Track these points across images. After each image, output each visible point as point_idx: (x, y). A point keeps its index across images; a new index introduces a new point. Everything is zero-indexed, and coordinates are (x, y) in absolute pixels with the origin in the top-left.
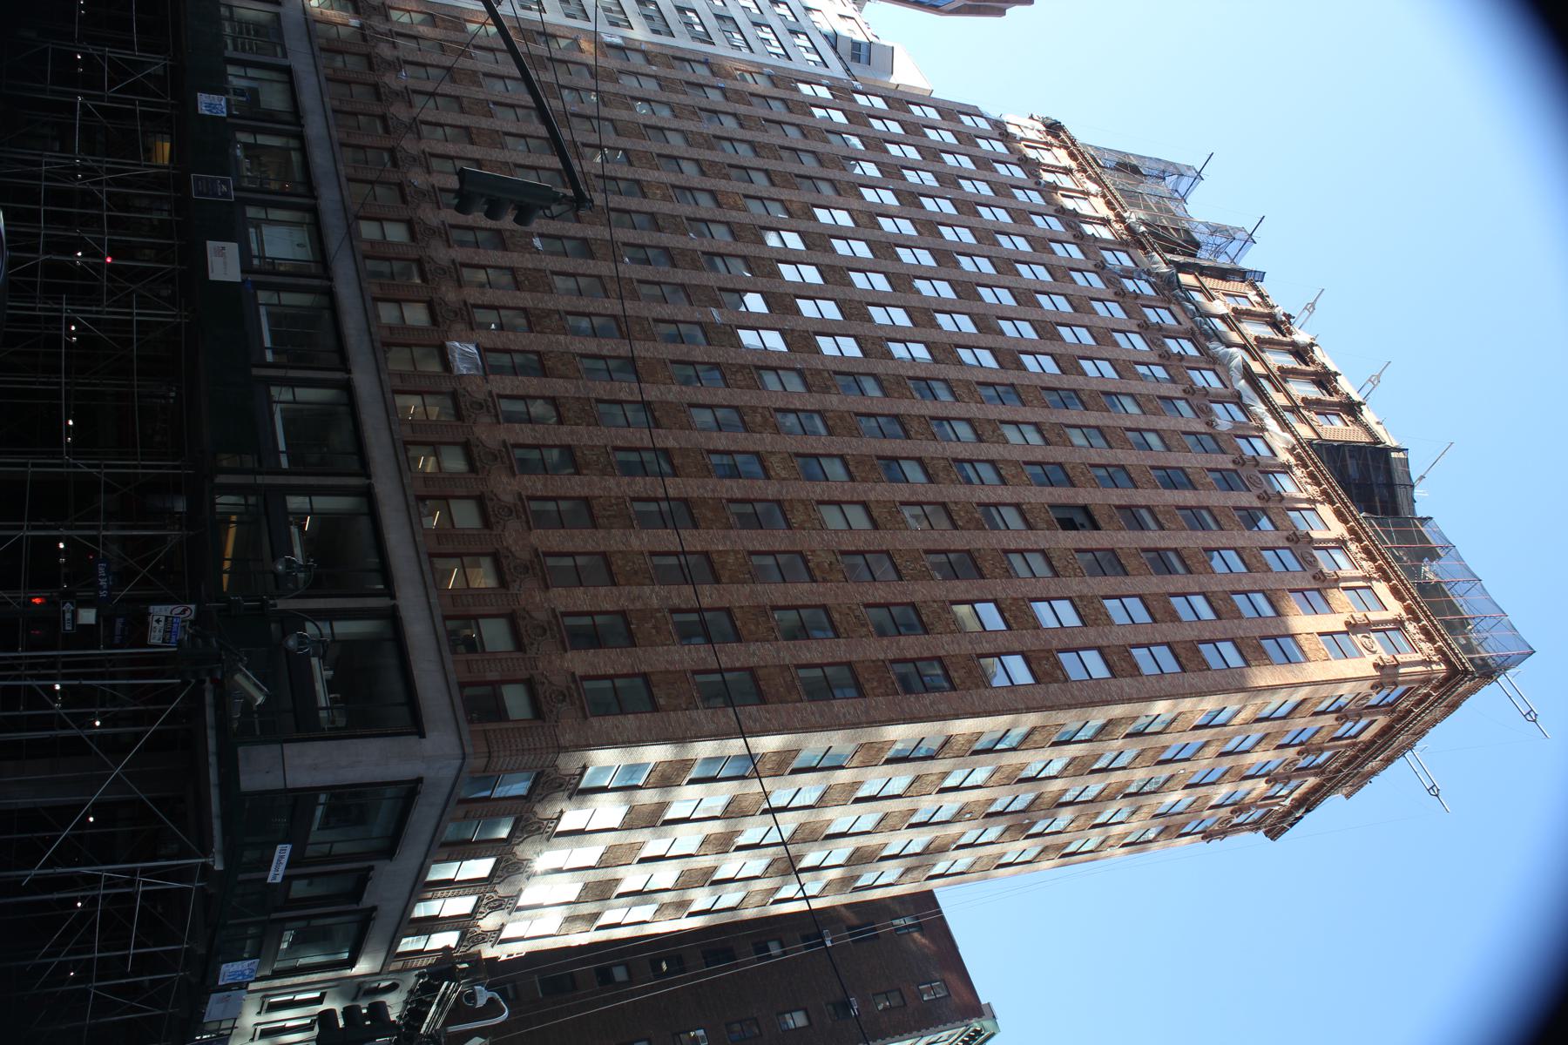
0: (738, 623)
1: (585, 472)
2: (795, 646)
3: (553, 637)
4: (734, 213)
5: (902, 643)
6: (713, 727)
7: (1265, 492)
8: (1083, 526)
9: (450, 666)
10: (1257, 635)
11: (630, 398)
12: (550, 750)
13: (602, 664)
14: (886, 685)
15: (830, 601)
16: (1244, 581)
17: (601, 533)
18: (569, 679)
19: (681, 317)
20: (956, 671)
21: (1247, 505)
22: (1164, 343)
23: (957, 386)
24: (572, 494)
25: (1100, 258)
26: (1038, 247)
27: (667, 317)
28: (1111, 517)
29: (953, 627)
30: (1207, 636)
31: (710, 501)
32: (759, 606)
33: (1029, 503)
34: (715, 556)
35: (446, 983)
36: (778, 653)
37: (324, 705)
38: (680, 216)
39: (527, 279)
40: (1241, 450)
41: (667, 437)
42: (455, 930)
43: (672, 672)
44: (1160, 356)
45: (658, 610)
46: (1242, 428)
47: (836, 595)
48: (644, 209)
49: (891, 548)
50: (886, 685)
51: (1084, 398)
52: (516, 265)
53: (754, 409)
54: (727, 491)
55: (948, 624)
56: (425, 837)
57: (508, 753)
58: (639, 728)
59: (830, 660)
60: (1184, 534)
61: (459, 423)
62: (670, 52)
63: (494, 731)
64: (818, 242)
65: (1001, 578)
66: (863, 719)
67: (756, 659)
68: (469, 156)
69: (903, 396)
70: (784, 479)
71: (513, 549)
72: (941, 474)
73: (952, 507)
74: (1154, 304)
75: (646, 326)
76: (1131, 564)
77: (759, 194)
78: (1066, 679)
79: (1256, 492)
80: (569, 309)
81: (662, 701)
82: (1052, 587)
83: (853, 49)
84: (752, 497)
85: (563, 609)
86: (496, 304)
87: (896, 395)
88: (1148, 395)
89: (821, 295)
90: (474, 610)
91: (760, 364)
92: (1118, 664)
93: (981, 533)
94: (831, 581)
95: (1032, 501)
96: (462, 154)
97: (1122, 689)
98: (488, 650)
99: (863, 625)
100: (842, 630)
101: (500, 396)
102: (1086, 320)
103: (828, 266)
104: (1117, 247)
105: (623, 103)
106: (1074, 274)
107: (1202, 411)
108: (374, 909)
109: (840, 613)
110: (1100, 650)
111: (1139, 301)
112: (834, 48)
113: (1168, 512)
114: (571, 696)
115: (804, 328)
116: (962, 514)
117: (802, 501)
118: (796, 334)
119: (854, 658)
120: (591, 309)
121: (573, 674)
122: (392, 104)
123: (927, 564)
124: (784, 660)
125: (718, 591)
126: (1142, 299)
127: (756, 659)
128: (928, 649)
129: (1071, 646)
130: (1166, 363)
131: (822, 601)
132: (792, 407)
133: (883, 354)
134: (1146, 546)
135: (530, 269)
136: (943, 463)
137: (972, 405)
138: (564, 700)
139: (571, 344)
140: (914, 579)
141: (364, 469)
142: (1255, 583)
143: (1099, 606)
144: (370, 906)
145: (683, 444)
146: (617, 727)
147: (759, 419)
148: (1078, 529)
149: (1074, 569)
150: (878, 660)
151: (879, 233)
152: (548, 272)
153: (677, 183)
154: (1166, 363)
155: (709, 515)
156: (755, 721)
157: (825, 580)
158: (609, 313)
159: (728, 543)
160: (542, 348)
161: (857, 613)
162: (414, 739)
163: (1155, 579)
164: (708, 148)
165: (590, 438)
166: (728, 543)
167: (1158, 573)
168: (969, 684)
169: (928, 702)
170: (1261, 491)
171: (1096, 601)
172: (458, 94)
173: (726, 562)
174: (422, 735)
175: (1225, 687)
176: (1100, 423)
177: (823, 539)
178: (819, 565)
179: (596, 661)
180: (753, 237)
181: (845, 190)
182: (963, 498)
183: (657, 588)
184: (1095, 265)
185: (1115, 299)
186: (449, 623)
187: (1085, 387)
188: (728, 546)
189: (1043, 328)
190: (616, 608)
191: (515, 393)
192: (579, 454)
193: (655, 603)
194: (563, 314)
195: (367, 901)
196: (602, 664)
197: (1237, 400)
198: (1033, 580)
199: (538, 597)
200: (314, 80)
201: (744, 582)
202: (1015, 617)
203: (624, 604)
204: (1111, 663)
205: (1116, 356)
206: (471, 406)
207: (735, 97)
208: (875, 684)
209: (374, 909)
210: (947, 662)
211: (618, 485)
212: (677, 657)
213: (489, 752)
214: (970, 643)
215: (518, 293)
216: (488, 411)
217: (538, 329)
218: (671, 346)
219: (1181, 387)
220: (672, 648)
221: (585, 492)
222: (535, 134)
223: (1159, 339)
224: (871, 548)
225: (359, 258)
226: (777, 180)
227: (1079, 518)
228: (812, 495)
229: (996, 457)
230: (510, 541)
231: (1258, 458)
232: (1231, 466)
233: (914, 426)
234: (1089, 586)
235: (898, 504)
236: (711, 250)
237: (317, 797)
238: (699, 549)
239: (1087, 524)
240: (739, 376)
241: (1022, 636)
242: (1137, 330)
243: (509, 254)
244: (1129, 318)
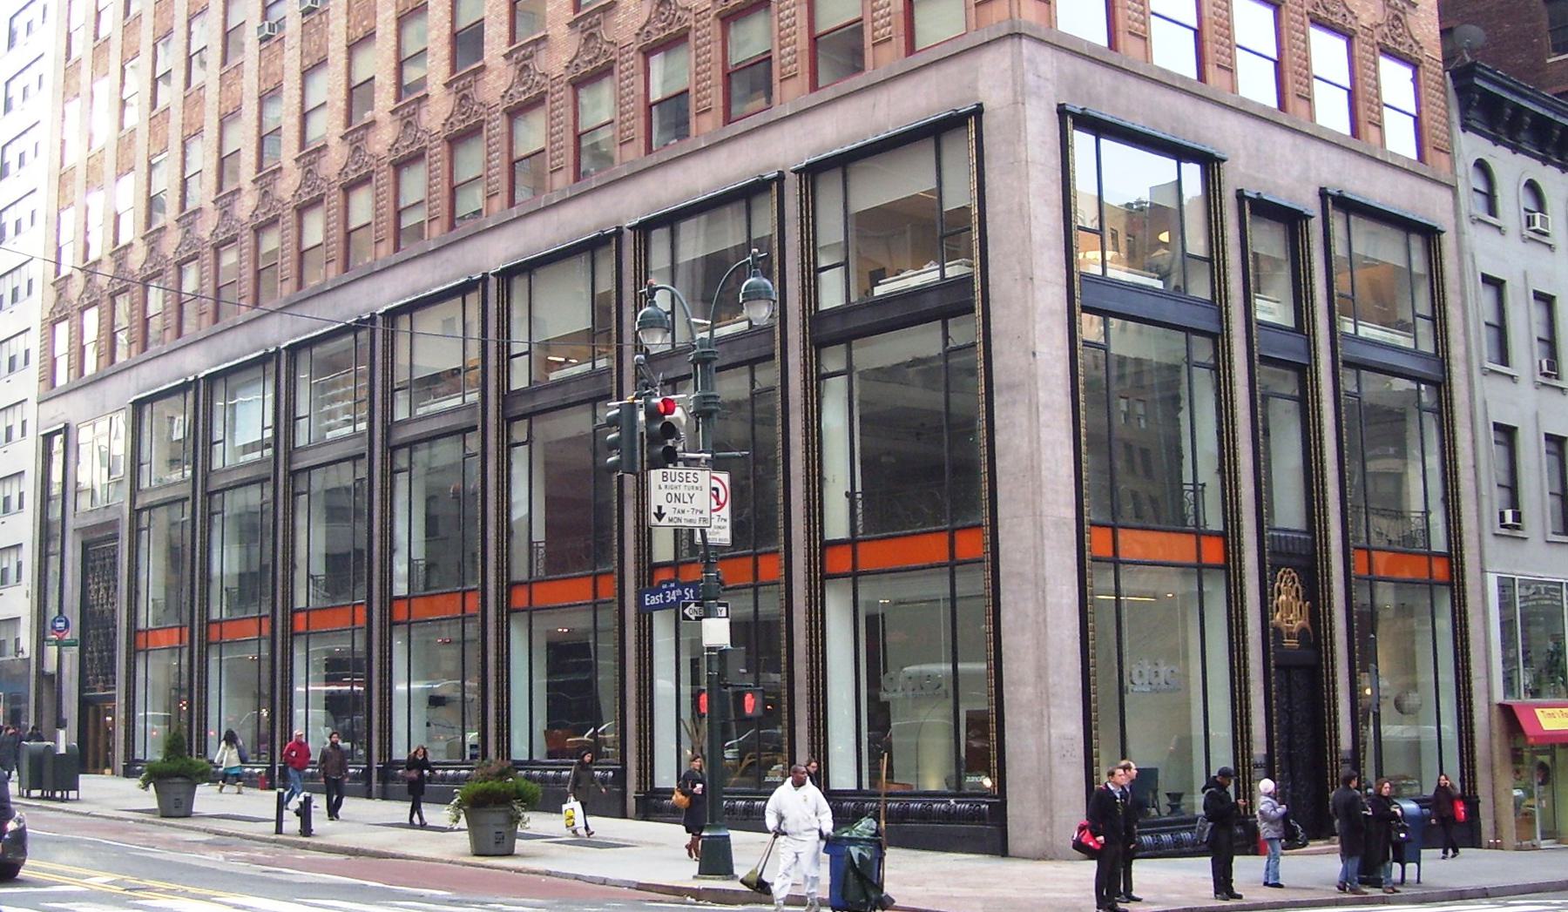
35: (1477, 81)
42: (1376, 63)
52: (344, 42)
56: (1183, 104)
68: (216, 135)
86: (393, 65)
90: (803, 42)
101: (512, 40)
108: (1323, 194)
122: (164, 257)
135: (348, 21)
144: (1318, 198)
162: (987, 121)
191: (506, 18)
195: (1309, 202)
206: (525, 84)
209: (1323, 194)
215: (377, 35)
222: (185, 41)
243: (331, 54)
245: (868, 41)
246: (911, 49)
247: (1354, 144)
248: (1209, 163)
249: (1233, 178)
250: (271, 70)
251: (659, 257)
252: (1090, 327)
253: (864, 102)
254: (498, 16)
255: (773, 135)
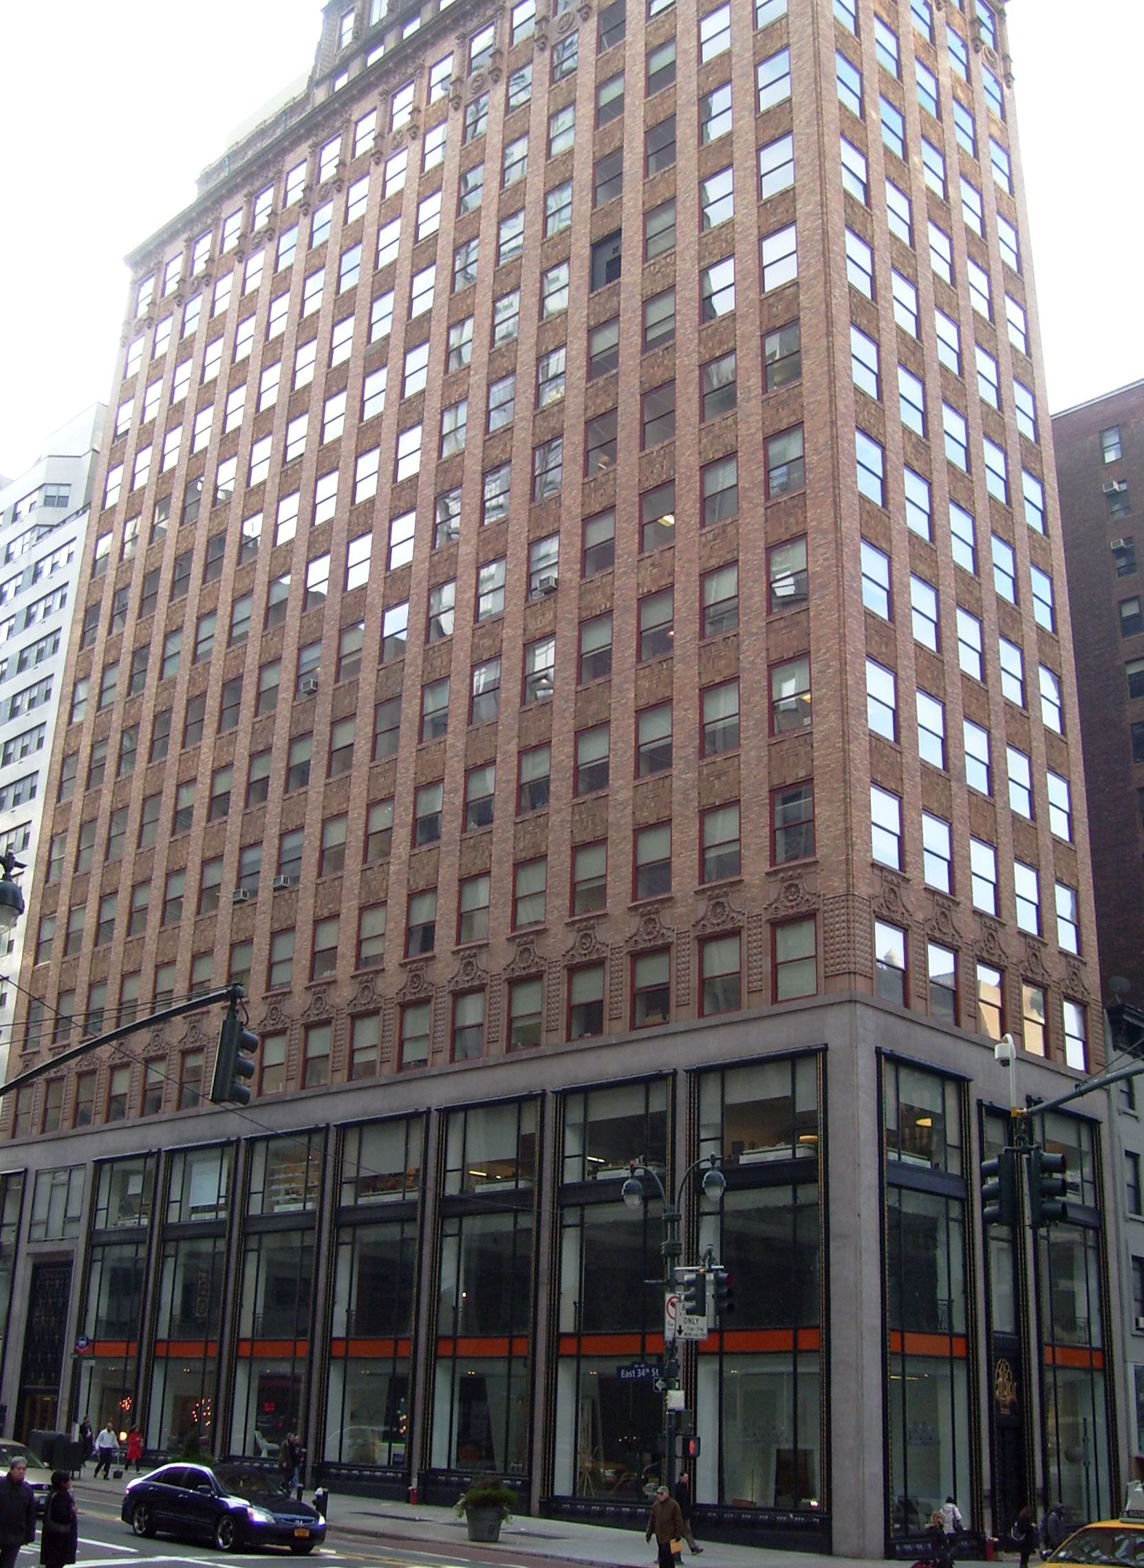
0: (718, 680)
1: (543, 849)
2: (744, 615)
3: (726, 894)
4: (249, 660)
5: (747, 486)
6: (833, 717)
7: (579, 11)
8: (617, 249)
9: (754, 1013)
10: (751, 33)
11: (462, 792)
12: (851, 904)
13: (758, 841)
14: (794, 507)
15: (696, 570)
16: (686, 46)
17: (613, 835)
18: (772, 879)
19: (369, 729)
20: (781, 421)
21: (594, 35)
22: (399, 132)
23: (449, 398)
24: (568, 864)
25: (296, 208)
26: (284, 286)
27: (370, 745)
28: (606, 214)
29: (730, 421)
30: (750, 100)
31: (579, 704)
32: (700, 655)
33: (588, 316)
34: (642, 702)
35: (1125, 1017)
36: (754, 634)
37: (790, 1151)
38: (254, 724)
39: (326, 905)
40: (529, 38)
41: (505, 753)
42: (1062, 1007)
43: (770, 760)
44: (414, 138)
45: (700, 773)
46: (501, 36)
47: (689, 561)
48: (246, 766)
49: (636, 492)
50: (794, 507)
51: (464, 239)
52: (311, 917)
53: (474, 647)
54: (567, 684)
55: (726, 427)
56: (948, 1042)
57: (851, 952)
58: (830, 802)
59: (763, 573)
60: (628, 121)
61: (488, 989)
62: (64, 727)
63: (826, 966)
64: (281, 560)
65: (675, 358)
66: (831, 537)
67: (758, 661)
69: (461, 467)
70: (555, 617)
71: (629, 935)
72: (552, 424)
73: (590, 414)
74: (351, 142)
75: (379, 770)
76: (663, 193)
77: (227, 628)
78: (795, 283)
79: (578, 23)
80: (360, 858)
81: (802, 774)
82: (687, 294)
83: (53, 505)
84: (576, 655)
85: (697, 881)
86: (355, 941)
87: (459, 474)
88: (461, 157)
89: (343, 560)
90: (695, 982)
91: (423, 637)
92: (779, 217)
93: (622, 379)
94: (673, 565)
95: (585, 313)
96: (187, 974)
97: (809, 214)
98: (737, 969)
99: (724, 531)
100: (729, 557)
102: (370, 230)
103: (309, 550)
104: (283, 185)
105: (124, 785)
106: (316, 244)
107: (480, 87)
109: (710, 557)
110: (763, 237)
111: (348, 161)
112: (52, 528)
113: (602, 140)
114: (791, 878)
115: (381, 582)
116: (599, 401)
117: (581, 596)
118: (388, 592)
119: (762, 544)
120: (361, 833)
121: (768, 874)
123: (657, 448)
124: (760, 628)
125: (680, 701)
126: (345, 155)
127: (758, 661)
128: (754, 453)
129: (757, 275)
130: (422, 131)
131: (695, 578)
132: (472, 602)
133: (411, 487)
134: (641, 171)
136: (539, 422)
137: (472, 380)
138: (796, 886)
139: (400, 858)
140: (673, 463)
141: (538, 1098)
142: (689, 32)
143: (710, 237)
145: (515, 733)
146: (828, 826)
147: (487, 642)
148: (619, 257)
149: (667, 265)
150: (765, 514)
151: (269, 485)
152: (319, 881)
153: (215, 725)
154: (422, 131)
155: (594, 707)
156: (829, 667)
157: (672, 574)
158: (364, 813)
159: (626, 686)
160: (405, 892)
161: (710, 536)
163: (681, 162)
164: (174, 687)
165: (505, 841)
166: (626, 686)
167: (673, 158)
168: (796, 406)
169: (815, 458)
170: (578, 16)
171: (704, 240)
172: (119, 976)
173: (649, 690)
174: (825, 1049)
175: (812, 80)
176: (494, 220)
177: (625, 573)
178: (654, 580)
179: (753, 847)
180: (276, 639)
181: (221, 524)
182: (581, 399)
183: (675, 772)
184: (305, 215)
185: (345, 192)
186: (706, 1011)
187: (452, 236)
188: (631, 686)
189: (381, 286)
190: (697, 822)
191: (454, 924)
192: (523, 855)
193: (691, 775)
194: (366, 866)
196: (758, 841)
197: (467, 40)
198: (678, 318)
199: (680, 910)
200: (109, 1136)
201: (671, 669)
202: (721, 342)
203: (692, 811)
204: (777, 226)
205: (415, 195)
207: (113, 653)
208: (792, 520)
210: (770, 431)
211: (559, 811)
212: (753, 753)
213: (850, 973)
214: (749, 400)
216: (475, 956)
217: (382, 895)
218: (402, 742)
219: (452, 113)
220: (742, 758)
221: (566, 850)
223: (394, 138)
224: (637, 515)
225: (304, 1094)
226: (209, 606)
227: (607, 254)
228: (574, 584)
229: (533, 355)
230: (619, 937)
231: (538, 17)
232: (547, 53)
233: (497, 454)
234: (686, 248)
235: (586, 480)
236: (292, 689)
237: (891, 1163)
238: (632, 721)
239: (614, 245)
240: (437, 663)
241: (743, 336)
242: (382, 165)
244: (368, 174)
245: (744, 990)
246: (775, 1000)
247: (1046, 1063)
248: (961, 1083)
249: (977, 1091)
250: (242, 925)
251: (575, 1115)
252: (891, 1199)
253: (739, 1031)
254: (448, 922)
255: (669, 1042)
